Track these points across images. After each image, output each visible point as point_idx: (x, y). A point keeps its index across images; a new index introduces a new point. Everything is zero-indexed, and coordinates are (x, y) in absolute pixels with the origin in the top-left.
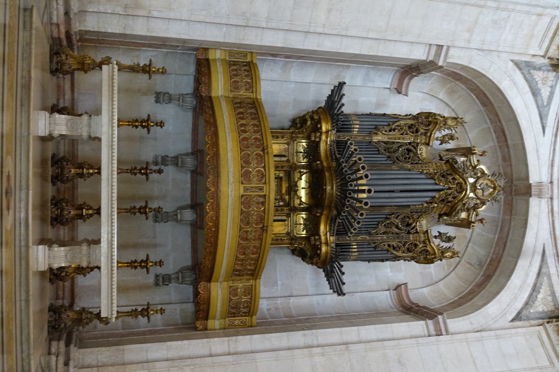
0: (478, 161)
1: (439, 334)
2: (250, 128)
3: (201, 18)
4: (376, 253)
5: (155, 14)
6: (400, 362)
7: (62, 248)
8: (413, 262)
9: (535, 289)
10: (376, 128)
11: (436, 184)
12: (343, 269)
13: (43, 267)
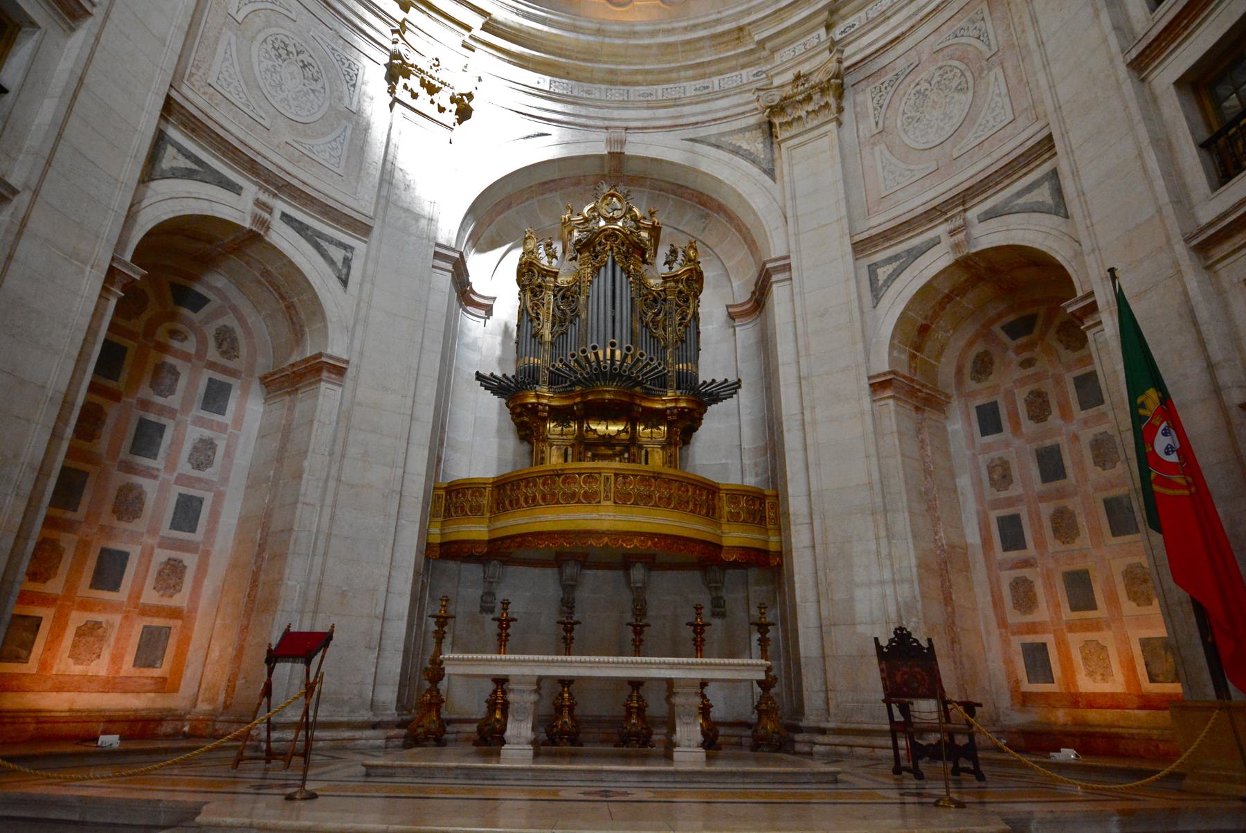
1: (788, 268)
2: (530, 492)
3: (388, 551)
4: (688, 340)
5: (380, 609)
7: (678, 729)
8: (701, 297)
9: (736, 151)
10: (534, 336)
12: (709, 381)
13: (701, 754)
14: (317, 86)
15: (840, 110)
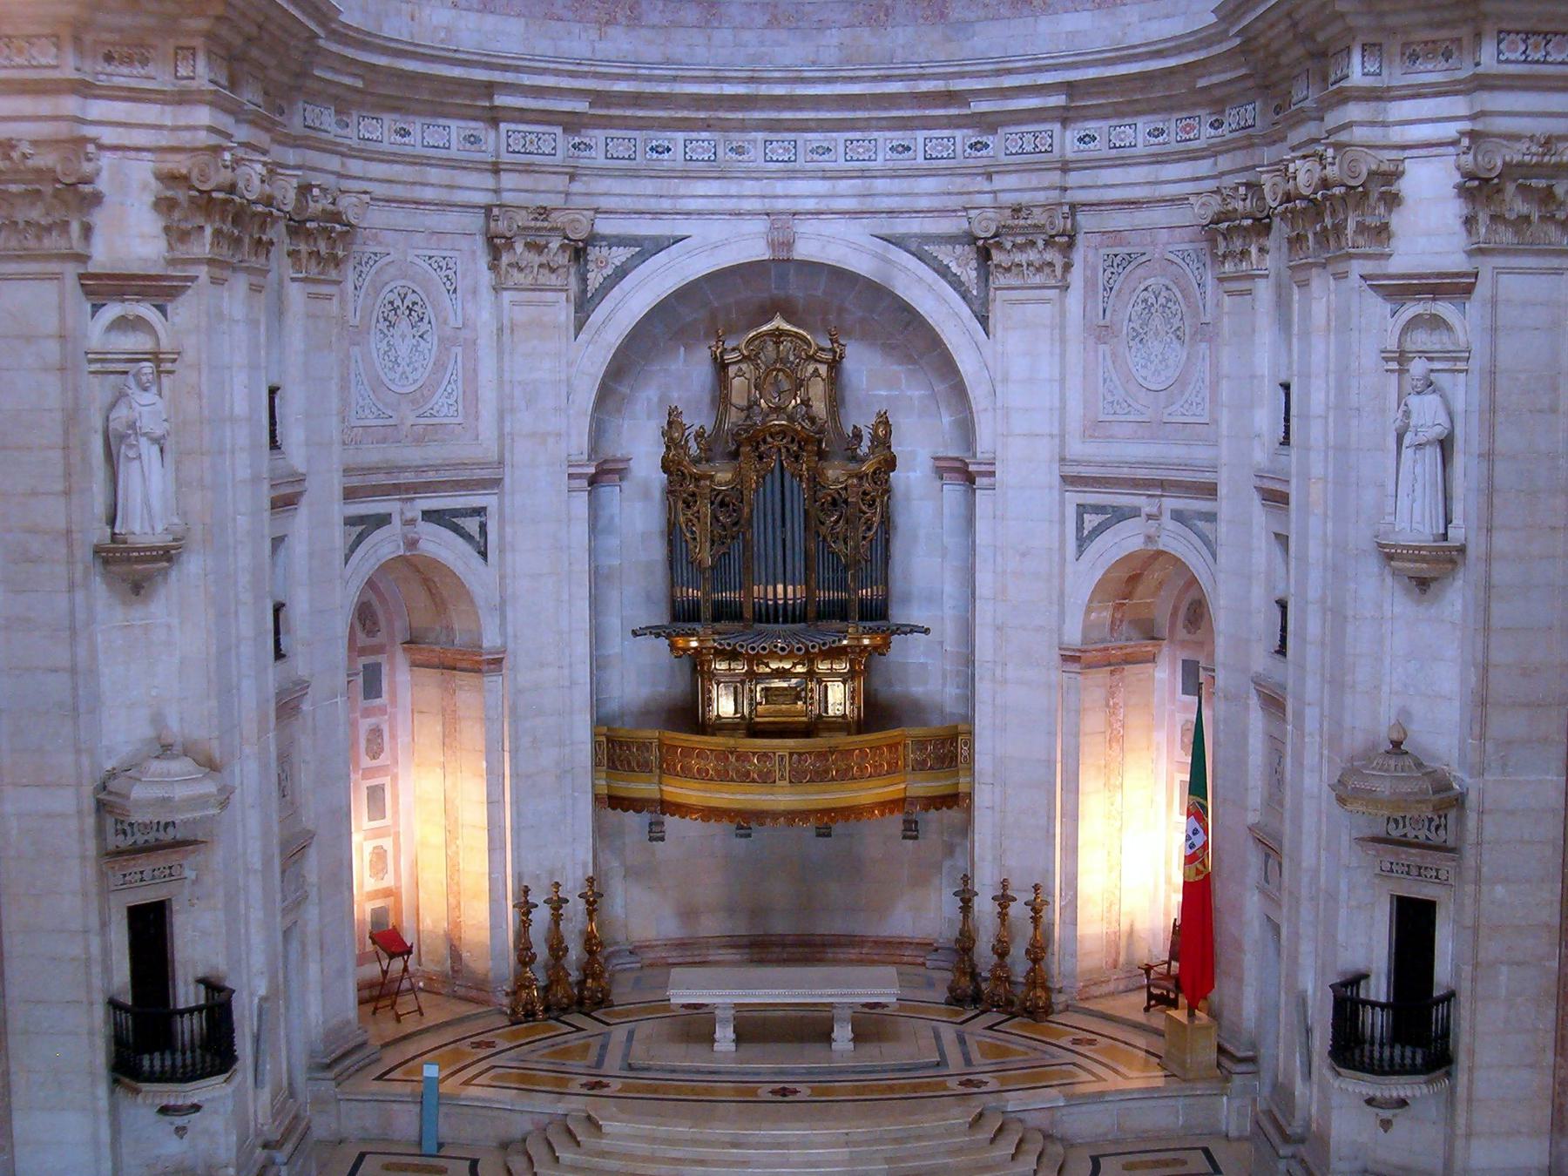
0: (733, 350)
6: (1023, 555)
9: (943, 272)
11: (772, 471)
14: (424, 326)
15: (1067, 267)
